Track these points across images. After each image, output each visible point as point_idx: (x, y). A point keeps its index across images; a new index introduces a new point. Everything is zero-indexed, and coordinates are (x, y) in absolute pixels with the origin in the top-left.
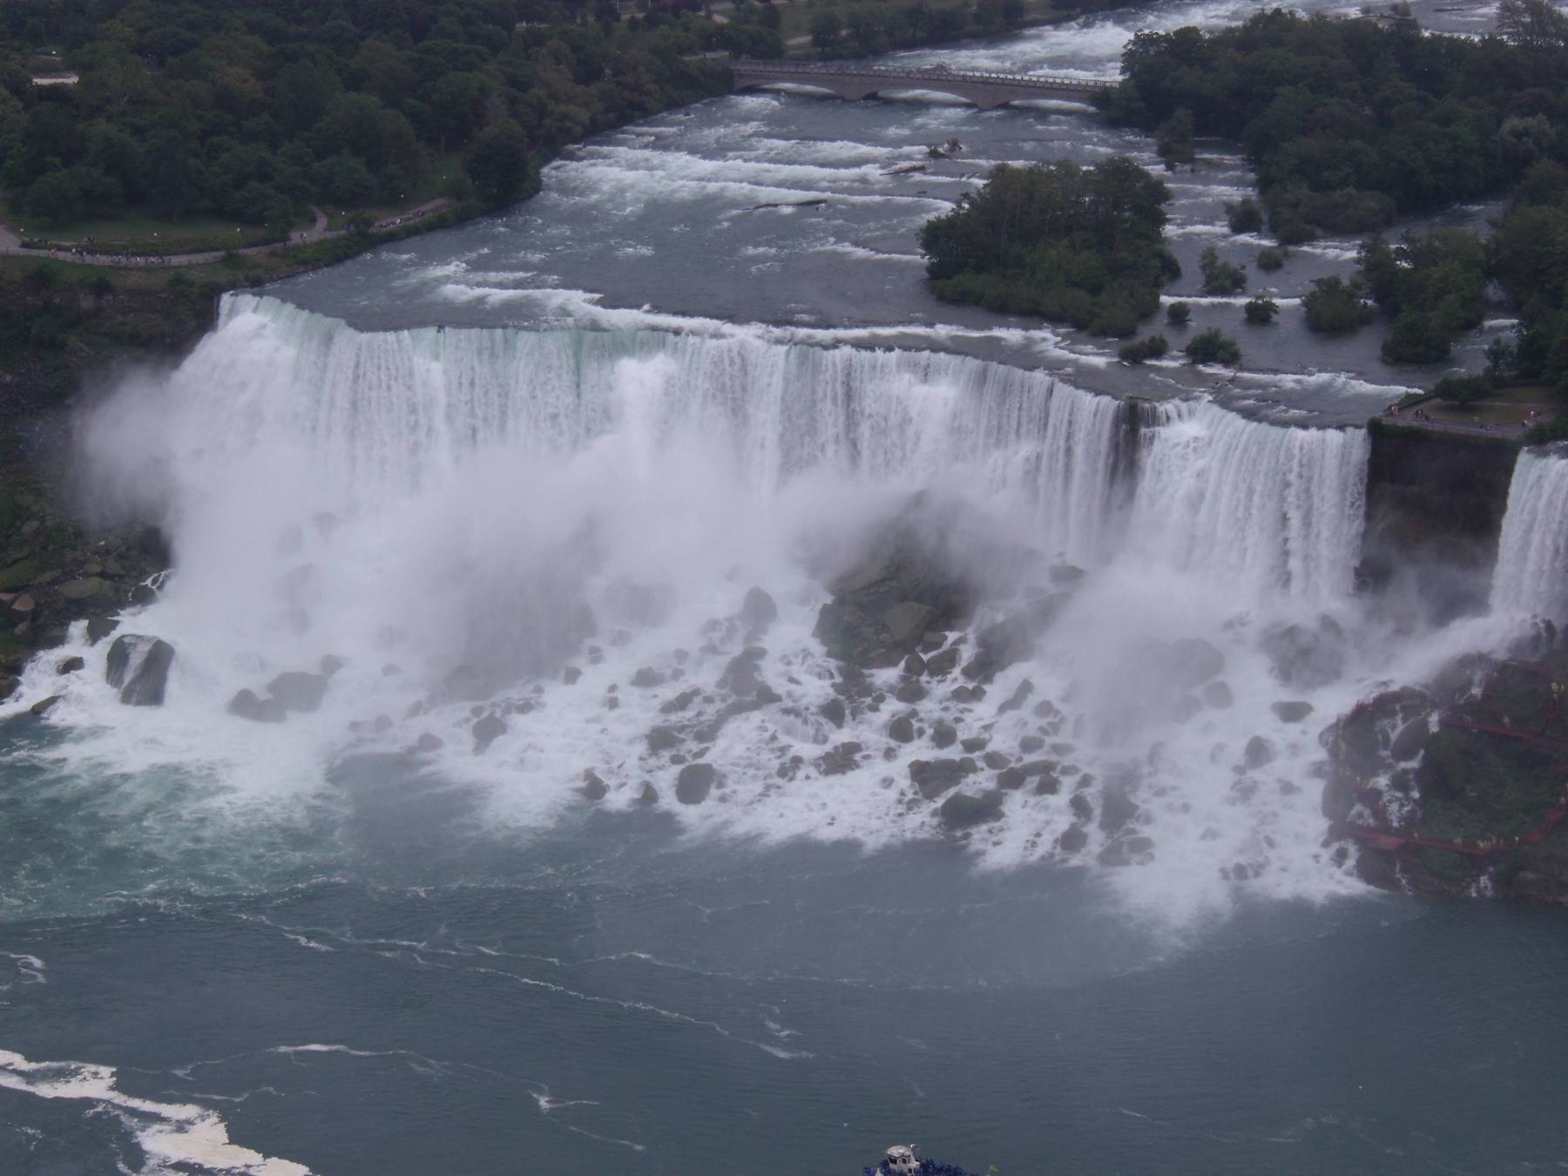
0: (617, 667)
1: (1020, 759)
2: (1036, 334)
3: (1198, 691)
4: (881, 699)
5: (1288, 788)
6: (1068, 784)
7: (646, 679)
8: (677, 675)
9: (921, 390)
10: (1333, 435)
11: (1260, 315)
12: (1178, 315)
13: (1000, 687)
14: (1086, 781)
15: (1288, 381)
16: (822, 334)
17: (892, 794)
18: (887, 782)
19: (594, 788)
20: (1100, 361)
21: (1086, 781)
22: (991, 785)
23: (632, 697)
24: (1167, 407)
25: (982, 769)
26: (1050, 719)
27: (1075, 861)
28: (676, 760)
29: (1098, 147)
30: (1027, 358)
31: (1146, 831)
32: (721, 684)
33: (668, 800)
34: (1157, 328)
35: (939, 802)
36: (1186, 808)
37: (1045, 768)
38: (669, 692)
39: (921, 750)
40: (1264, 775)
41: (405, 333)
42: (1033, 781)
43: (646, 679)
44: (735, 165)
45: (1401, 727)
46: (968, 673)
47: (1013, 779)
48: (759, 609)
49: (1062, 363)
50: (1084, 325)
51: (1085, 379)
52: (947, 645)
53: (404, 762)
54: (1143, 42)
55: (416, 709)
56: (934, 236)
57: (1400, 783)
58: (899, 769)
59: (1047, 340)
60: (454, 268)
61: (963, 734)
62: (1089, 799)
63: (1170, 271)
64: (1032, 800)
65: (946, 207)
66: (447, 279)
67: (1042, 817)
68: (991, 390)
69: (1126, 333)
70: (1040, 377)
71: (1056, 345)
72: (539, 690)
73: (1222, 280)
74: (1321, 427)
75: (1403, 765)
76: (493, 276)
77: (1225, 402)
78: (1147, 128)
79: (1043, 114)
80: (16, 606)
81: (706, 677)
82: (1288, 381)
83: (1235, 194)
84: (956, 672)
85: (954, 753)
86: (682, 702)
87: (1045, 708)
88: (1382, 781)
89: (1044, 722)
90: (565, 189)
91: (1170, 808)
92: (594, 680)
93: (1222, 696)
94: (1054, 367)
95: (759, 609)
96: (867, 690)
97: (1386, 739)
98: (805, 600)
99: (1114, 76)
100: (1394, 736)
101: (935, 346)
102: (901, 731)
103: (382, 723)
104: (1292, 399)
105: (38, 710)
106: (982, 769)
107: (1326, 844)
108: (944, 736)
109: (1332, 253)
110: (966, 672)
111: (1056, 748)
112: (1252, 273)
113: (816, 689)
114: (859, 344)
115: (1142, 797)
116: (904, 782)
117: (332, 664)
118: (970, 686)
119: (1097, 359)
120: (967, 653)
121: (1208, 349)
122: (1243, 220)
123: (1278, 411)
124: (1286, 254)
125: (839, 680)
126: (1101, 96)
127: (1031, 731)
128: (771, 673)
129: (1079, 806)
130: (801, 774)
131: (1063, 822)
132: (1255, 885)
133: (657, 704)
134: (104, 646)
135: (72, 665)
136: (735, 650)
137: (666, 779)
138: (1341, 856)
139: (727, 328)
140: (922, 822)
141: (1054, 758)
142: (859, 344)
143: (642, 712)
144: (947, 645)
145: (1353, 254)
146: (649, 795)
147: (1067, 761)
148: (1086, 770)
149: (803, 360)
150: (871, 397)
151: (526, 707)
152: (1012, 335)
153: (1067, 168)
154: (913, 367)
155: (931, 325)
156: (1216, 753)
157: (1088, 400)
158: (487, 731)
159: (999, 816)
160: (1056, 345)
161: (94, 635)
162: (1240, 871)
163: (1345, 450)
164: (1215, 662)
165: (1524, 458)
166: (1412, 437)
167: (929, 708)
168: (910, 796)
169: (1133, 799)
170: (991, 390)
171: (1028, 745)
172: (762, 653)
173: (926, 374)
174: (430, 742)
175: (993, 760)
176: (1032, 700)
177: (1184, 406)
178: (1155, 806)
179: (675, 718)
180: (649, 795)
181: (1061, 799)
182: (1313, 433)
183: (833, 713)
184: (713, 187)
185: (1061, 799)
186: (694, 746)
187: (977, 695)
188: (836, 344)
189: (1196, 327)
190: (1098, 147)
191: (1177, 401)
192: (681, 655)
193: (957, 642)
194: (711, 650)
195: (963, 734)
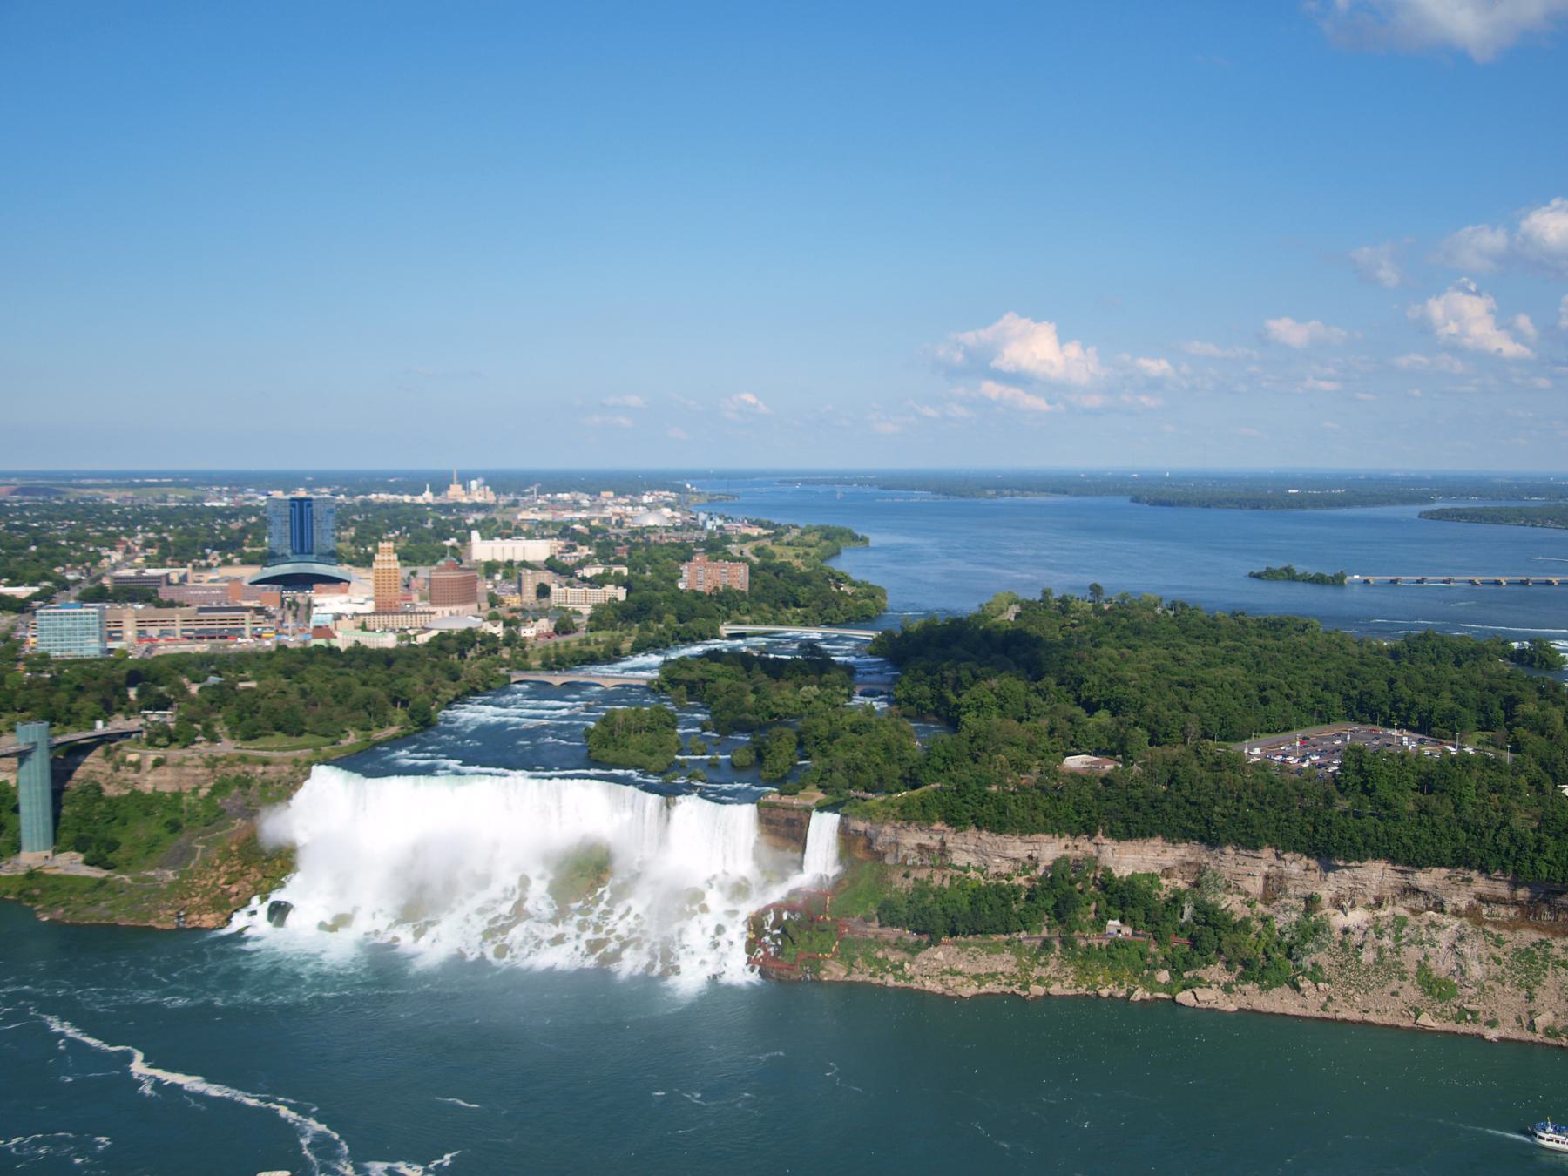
2: (629, 772)
3: (696, 908)
4: (573, 915)
7: (481, 911)
15: (726, 787)
17: (579, 953)
22: (618, 947)
23: (475, 918)
28: (494, 943)
30: (626, 781)
31: (677, 963)
33: (490, 956)
37: (638, 940)
39: (589, 935)
40: (723, 939)
44: (512, 710)
46: (607, 903)
47: (624, 945)
48: (525, 882)
49: (640, 782)
51: (648, 788)
52: (598, 894)
54: (665, 663)
55: (390, 927)
59: (633, 773)
60: (404, 752)
61: (606, 928)
66: (401, 757)
76: (421, 755)
77: (703, 795)
81: (506, 908)
82: (726, 787)
85: (602, 935)
86: (495, 920)
87: (637, 916)
88: (767, 938)
89: (636, 922)
90: (446, 720)
91: (686, 953)
95: (525, 882)
96: (569, 910)
98: (542, 877)
102: (582, 927)
103: (377, 932)
105: (241, 932)
108: (598, 928)
111: (642, 932)
113: (547, 912)
115: (677, 950)
116: (583, 947)
117: (355, 909)
120: (607, 896)
125: (556, 908)
127: (633, 926)
128: (528, 906)
129: (652, 954)
130: (543, 946)
131: (646, 960)
134: (267, 904)
135: (254, 913)
136: (517, 897)
138: (752, 970)
139: (511, 772)
140: (591, 962)
142: (561, 777)
143: (481, 924)
144: (598, 894)
146: (483, 956)
152: (620, 772)
155: (588, 769)
158: (419, 933)
159: (620, 959)
161: (264, 899)
167: (593, 917)
168: (586, 953)
171: (631, 931)
172: (526, 899)
175: (618, 938)
180: (483, 956)
183: (555, 921)
184: (503, 719)
186: (501, 937)
187: (610, 912)
188: (550, 778)
193: (603, 892)
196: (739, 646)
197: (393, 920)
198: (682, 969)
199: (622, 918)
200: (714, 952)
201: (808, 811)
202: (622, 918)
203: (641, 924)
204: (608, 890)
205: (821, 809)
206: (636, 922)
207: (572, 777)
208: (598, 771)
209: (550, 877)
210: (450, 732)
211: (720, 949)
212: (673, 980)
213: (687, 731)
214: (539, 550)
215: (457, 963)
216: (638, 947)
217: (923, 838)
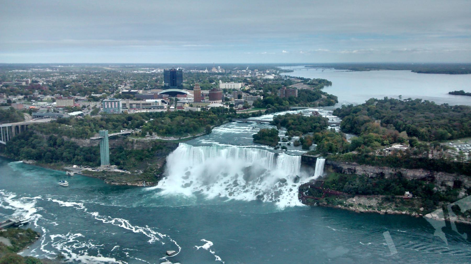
0: (222, 182)
2: (265, 146)
3: (284, 184)
4: (250, 185)
8: (228, 182)
9: (254, 152)
10: (298, 157)
11: (289, 144)
12: (280, 144)
13: (263, 183)
15: (292, 151)
16: (243, 146)
18: (251, 194)
19: (220, 194)
20: (272, 149)
24: (280, 154)
28: (229, 191)
29: (271, 127)
30: (265, 149)
32: (233, 183)
33: (228, 196)
34: (278, 146)
35: (257, 196)
38: (228, 184)
41: (199, 147)
43: (225, 183)
48: (237, 176)
50: (270, 145)
51: (271, 151)
53: (199, 192)
55: (200, 187)
56: (254, 136)
58: (252, 192)
59: (267, 147)
63: (279, 139)
65: (255, 133)
68: (261, 152)
69: (275, 146)
72: (213, 184)
73: (284, 140)
74: (296, 156)
76: (208, 141)
78: (276, 125)
79: (265, 124)
80: (158, 176)
81: (231, 182)
82: (292, 151)
83: (285, 132)
85: (258, 190)
86: (229, 185)
92: (219, 183)
93: (286, 184)
94: (267, 150)
95: (237, 176)
99: (272, 120)
101: (255, 148)
102: (252, 188)
104: (293, 153)
114: (247, 147)
119: (272, 149)
121: (283, 148)
122: (286, 135)
126: (270, 122)
128: (238, 182)
133: (226, 186)
136: (234, 180)
137: (227, 193)
139: (233, 146)
142: (247, 147)
149: (241, 149)
150: (248, 153)
151: (212, 186)
152: (263, 146)
153: (268, 129)
154: (252, 150)
158: (208, 189)
163: (299, 158)
164: (286, 181)
165: (318, 159)
166: (305, 157)
170: (261, 152)
173: (254, 150)
174: (202, 190)
175: (262, 191)
179: (228, 187)
182: (295, 156)
188: (244, 147)
189: (282, 145)
190: (271, 127)
192: (229, 180)
194: (232, 180)
196: (296, 112)
197: (201, 185)
201: (316, 158)
205: (319, 157)
207: (250, 148)
208: (257, 146)
209: (243, 174)
210: (216, 135)
212: (277, 203)
214: (238, 86)
215: (218, 198)
216: (268, 194)
217: (350, 167)
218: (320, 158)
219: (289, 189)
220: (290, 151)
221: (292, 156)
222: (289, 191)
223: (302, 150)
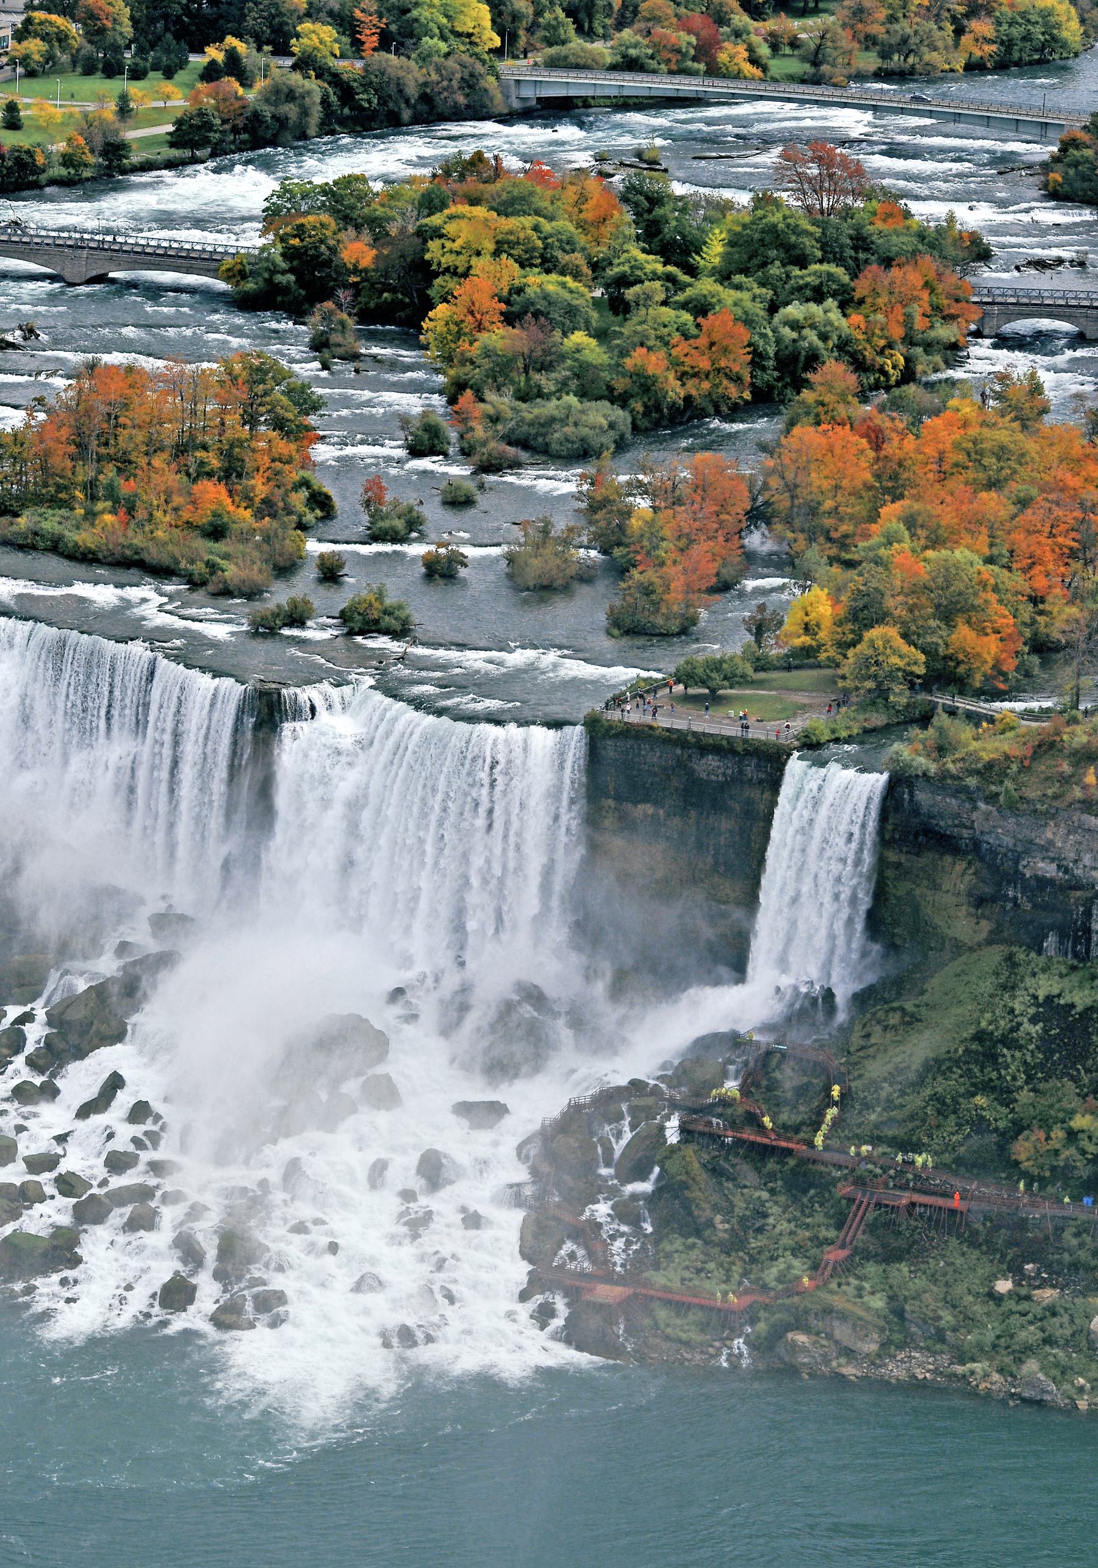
1: (104, 1183)
2: (133, 593)
5: (473, 1220)
6: (169, 1216)
10: (542, 738)
14: (195, 1212)
15: (475, 660)
20: (219, 632)
21: (195, 1212)
25: (52, 1197)
26: (149, 1126)
27: (179, 1323)
31: (277, 1282)
36: (333, 1248)
42: (120, 1215)
45: (628, 1136)
57: (625, 1212)
61: (26, 1147)
62: (200, 1237)
64: (122, 1239)
67: (135, 1263)
70: (138, 649)
71: (161, 608)
74: (523, 723)
75: (630, 1188)
77: (390, 689)
82: (475, 660)
84: (19, 1061)
87: (140, 1112)
88: (602, 1210)
91: (311, 1249)
94: (155, 638)
97: (609, 1151)
100: (619, 1148)
104: (482, 685)
106: (52, 1197)
107: (524, 1296)
109: (543, 485)
110: (30, 1062)
111: (155, 1167)
112: (433, 512)
118: (38, 1080)
123: (466, 702)
124: (481, 487)
127: (122, 1144)
131: (165, 1270)
132: (423, 1354)
138: (544, 1315)
141: (152, 1182)
145: (571, 488)
147: (168, 1185)
148: (194, 1197)
156: (377, 1172)
157: (205, 682)
159: (75, 1261)
160: (161, 608)
162: (406, 1336)
165: (795, 766)
169: (259, 1236)
171: (117, 1163)
175: (68, 1185)
176: (124, 1100)
177: (335, 693)
178: (293, 1248)
181: (160, 1239)
182: (512, 730)
185: (160, 1239)
191: (325, 686)
195: (26, 1147)
198: (292, 1309)
199: (85, 1111)
200: (408, 1251)
202: (85, 1111)
203: (154, 1138)
204: (41, 1014)
206: (138, 1130)
211: (432, 1240)
213: (349, 451)
218: (823, 764)
219: (413, 1159)
220: (453, 655)
221: (462, 727)
222: (417, 1183)
223: (605, 644)
